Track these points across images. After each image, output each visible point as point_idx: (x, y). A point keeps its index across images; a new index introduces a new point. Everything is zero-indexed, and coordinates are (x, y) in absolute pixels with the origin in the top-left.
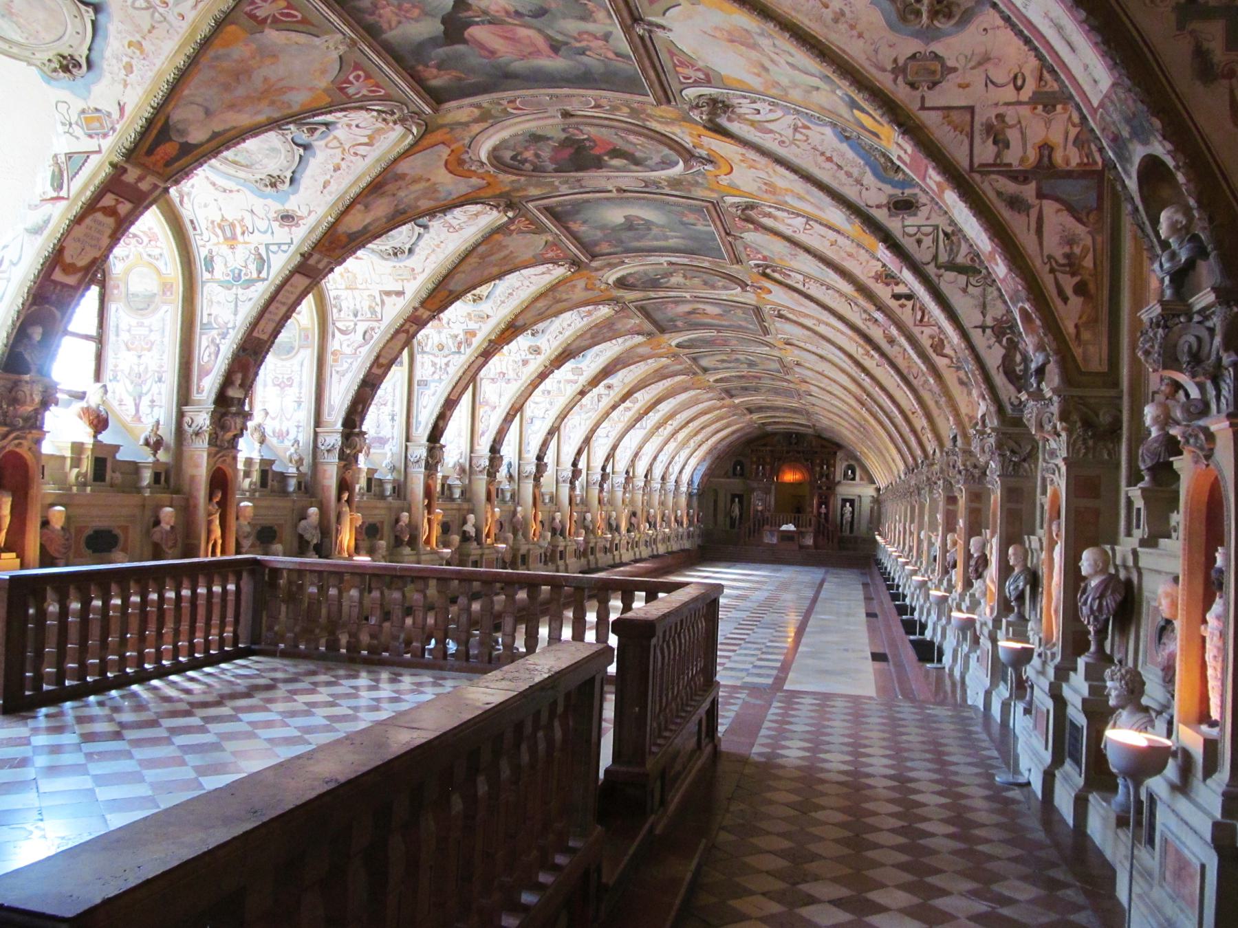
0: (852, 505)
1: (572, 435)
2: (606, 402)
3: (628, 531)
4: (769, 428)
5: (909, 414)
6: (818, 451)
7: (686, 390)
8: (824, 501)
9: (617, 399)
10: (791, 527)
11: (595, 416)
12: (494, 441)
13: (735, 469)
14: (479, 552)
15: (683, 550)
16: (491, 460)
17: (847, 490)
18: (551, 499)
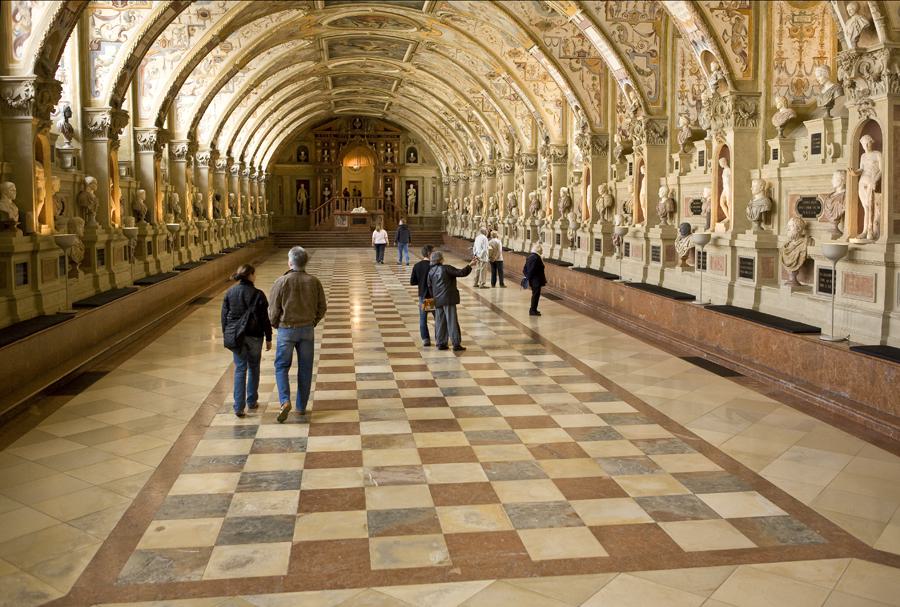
0: (416, 187)
1: (153, 83)
2: (199, 39)
3: (214, 216)
4: (336, 112)
5: (707, 11)
6: (383, 136)
7: (291, 36)
8: (388, 185)
9: (215, 33)
10: (362, 210)
11: (186, 57)
12: (43, 53)
13: (299, 154)
14: (29, 247)
15: (262, 238)
16: (38, 86)
17: (411, 172)
18: (129, 171)
